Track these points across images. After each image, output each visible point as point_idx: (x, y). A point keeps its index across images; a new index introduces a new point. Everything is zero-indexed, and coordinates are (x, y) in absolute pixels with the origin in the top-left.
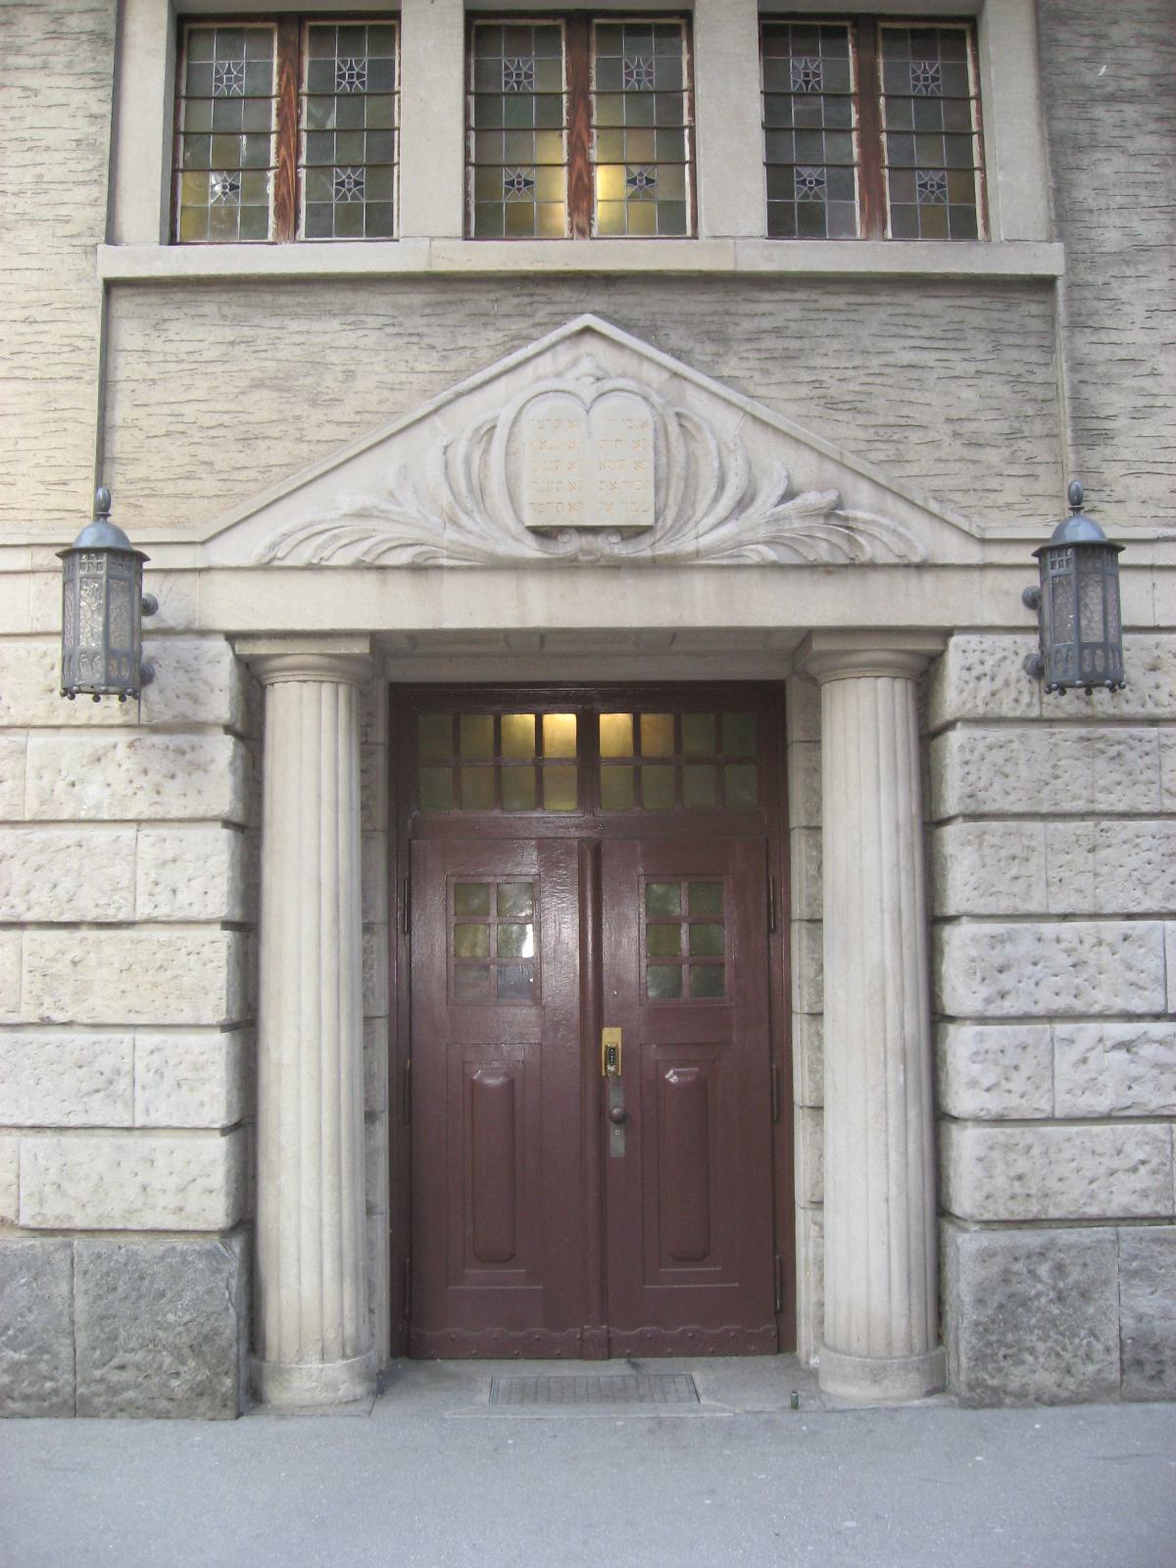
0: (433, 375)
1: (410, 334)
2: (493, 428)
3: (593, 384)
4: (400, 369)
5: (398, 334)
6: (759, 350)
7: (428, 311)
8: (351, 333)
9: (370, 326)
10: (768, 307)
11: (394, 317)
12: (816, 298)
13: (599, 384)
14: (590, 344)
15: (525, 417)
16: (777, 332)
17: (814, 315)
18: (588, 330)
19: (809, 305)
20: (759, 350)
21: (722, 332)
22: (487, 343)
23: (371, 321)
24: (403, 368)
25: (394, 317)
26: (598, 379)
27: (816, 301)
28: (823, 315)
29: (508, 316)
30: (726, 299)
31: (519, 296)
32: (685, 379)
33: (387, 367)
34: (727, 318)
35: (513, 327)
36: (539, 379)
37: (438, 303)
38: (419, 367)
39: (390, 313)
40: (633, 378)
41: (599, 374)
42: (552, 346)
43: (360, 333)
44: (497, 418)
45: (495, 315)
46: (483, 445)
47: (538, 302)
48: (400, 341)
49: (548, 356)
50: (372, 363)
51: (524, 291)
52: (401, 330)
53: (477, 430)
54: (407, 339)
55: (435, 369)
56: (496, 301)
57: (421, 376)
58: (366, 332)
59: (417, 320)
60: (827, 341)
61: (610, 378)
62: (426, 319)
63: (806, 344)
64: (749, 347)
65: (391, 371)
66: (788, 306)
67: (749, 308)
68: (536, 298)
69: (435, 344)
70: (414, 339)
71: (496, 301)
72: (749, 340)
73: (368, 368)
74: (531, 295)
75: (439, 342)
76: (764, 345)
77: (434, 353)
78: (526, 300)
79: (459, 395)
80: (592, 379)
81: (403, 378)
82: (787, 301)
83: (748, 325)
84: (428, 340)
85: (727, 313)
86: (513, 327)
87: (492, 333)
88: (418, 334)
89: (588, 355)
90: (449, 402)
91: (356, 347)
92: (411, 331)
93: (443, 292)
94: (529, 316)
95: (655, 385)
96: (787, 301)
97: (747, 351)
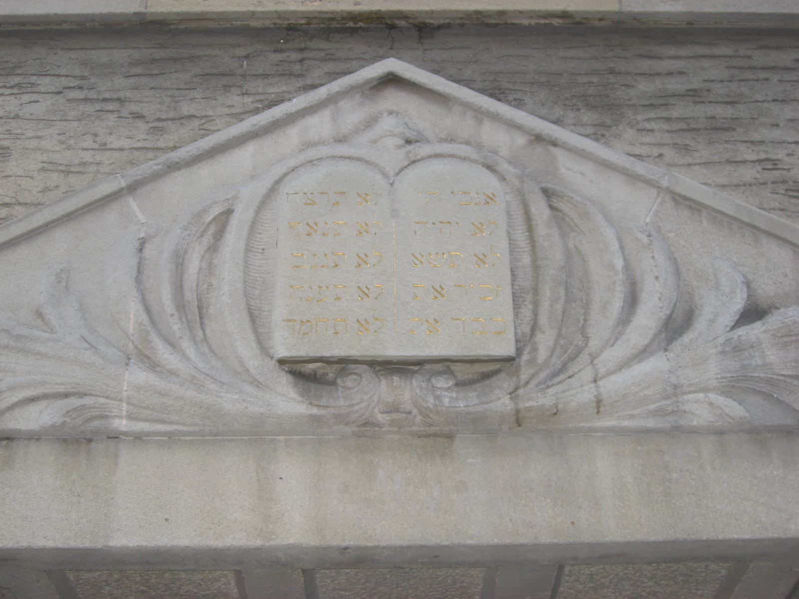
0: (136, 153)
1: (105, 100)
2: (229, 212)
3: (399, 147)
4: (85, 145)
5: (86, 100)
6: (668, 119)
7: (139, 70)
8: (13, 98)
9: (43, 90)
10: (679, 65)
11: (83, 78)
12: (749, 53)
13: (409, 148)
14: (393, 99)
15: (286, 188)
16: (694, 95)
17: (749, 75)
18: (391, 80)
19: (740, 62)
20: (668, 119)
21: (607, 96)
22: (227, 111)
23: (45, 83)
24: (89, 142)
25: (83, 78)
26: (408, 142)
27: (750, 57)
28: (762, 75)
29: (265, 76)
30: (610, 54)
31: (281, 51)
32: (554, 144)
33: (62, 142)
34: (612, 79)
35: (271, 90)
36: (309, 145)
37: (153, 61)
38: (115, 142)
39: (77, 72)
40: (468, 143)
41: (410, 135)
42: (331, 100)
43: (26, 98)
44: (235, 198)
45: (243, 76)
46: (208, 239)
47: (308, 59)
48: (89, 108)
49: (326, 114)
50: (38, 137)
51: (290, 45)
52: (92, 95)
53: (198, 216)
54: (98, 106)
55: (140, 145)
56: (247, 57)
57: (116, 154)
58: (35, 97)
59: (119, 81)
60: (775, 108)
61: (428, 141)
62: (132, 81)
63: (742, 111)
64: (652, 115)
65: (69, 148)
66: (706, 63)
67: (645, 65)
68: (306, 54)
69: (145, 112)
70: (110, 106)
71: (247, 57)
72: (652, 106)
73: (34, 143)
74: (302, 50)
75: (150, 109)
76: (675, 113)
77: (140, 124)
78: (294, 56)
79: (173, 167)
80: (400, 142)
81: (88, 156)
82: (704, 57)
83: (644, 86)
84: (133, 107)
85: (612, 72)
86: (271, 90)
87: (236, 98)
88: (119, 99)
89: (390, 113)
90: (156, 176)
91: (17, 117)
92: (107, 96)
93: (163, 47)
94: (299, 76)
95: (504, 152)
96: (704, 57)
97: (649, 120)
